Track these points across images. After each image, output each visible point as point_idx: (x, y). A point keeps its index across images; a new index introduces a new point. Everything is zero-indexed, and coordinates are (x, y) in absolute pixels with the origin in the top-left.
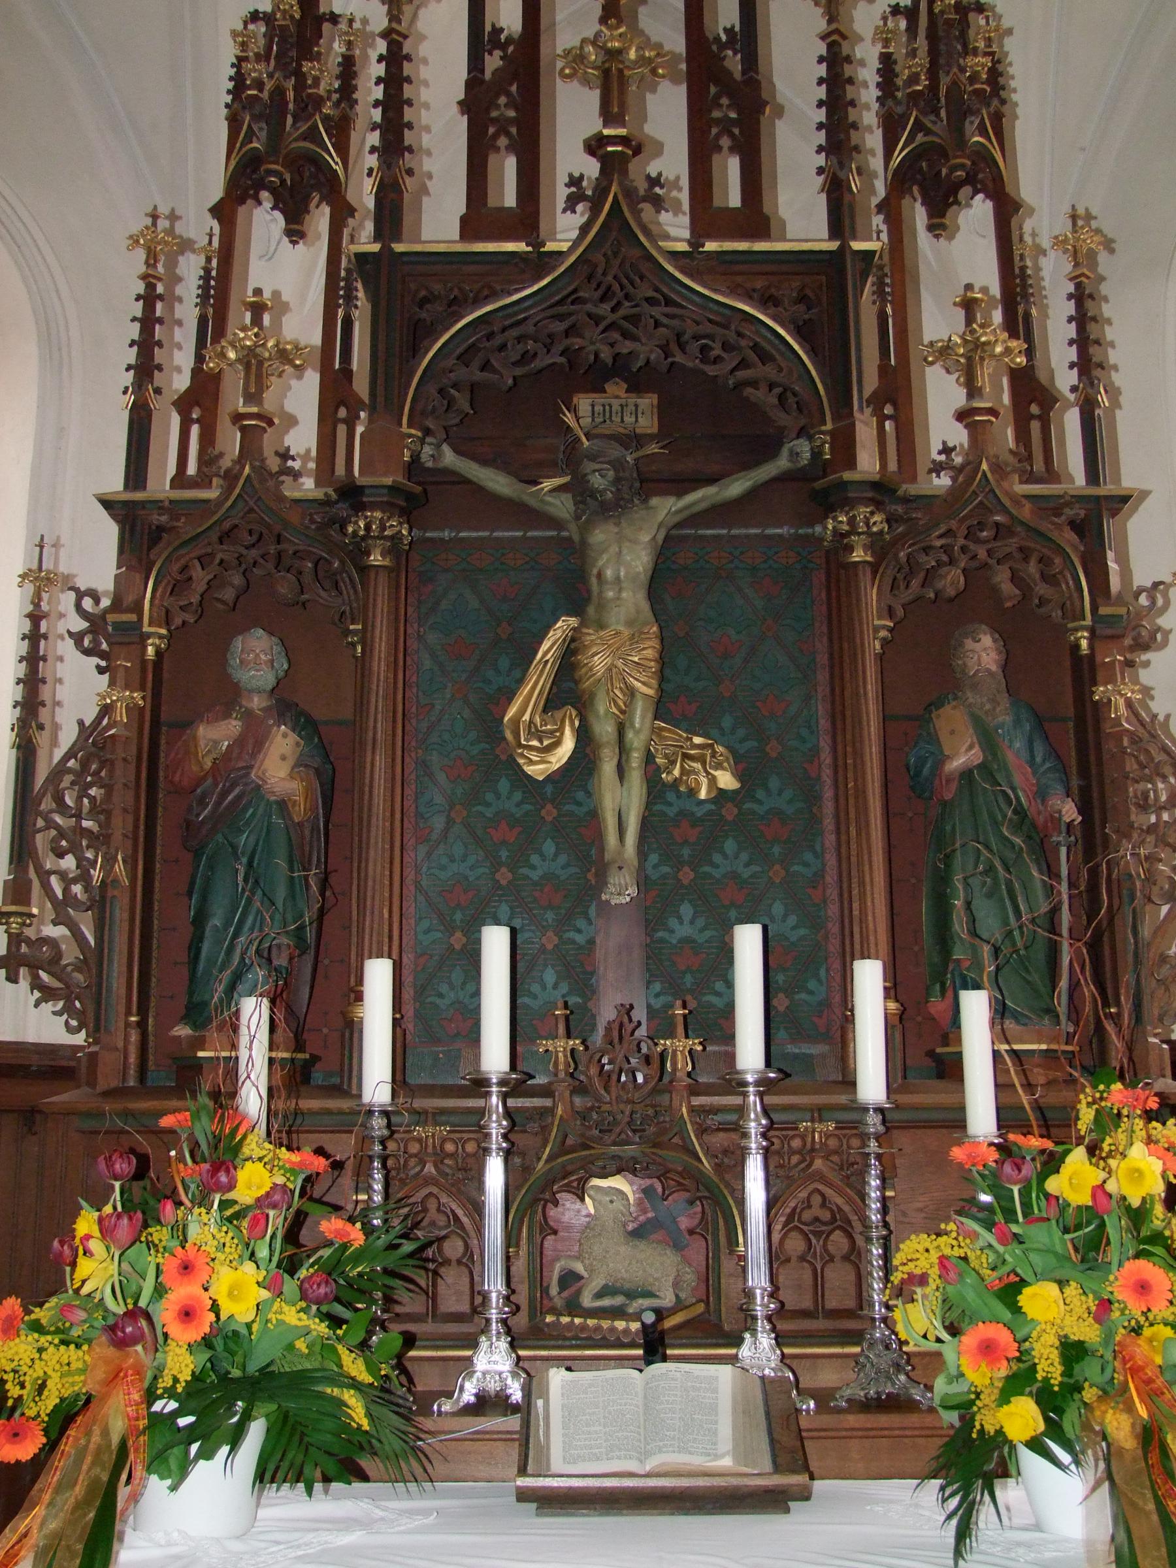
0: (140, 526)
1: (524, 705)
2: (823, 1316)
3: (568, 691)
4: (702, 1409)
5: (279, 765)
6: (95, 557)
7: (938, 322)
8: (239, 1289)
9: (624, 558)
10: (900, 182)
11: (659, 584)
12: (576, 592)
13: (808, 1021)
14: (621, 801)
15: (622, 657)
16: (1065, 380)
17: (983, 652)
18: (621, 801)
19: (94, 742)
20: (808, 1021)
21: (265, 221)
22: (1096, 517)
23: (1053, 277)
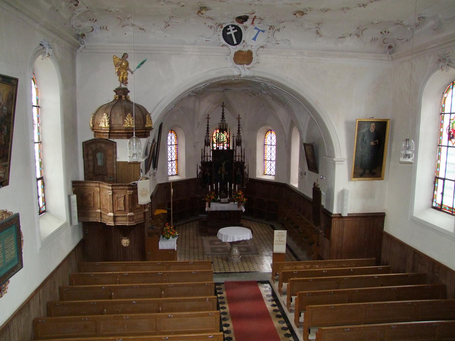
0: (202, 163)
1: (219, 171)
2: (231, 196)
3: (221, 170)
4: (226, 200)
5: (209, 175)
6: (200, 165)
7: (237, 155)
8: (213, 197)
9: (223, 164)
10: (236, 145)
11: (225, 166)
12: (221, 166)
13: (230, 186)
14: (223, 175)
15: (223, 170)
16: (243, 155)
17: (239, 169)
18: (223, 175)
19: (200, 173)
20: (230, 186)
21: (206, 147)
22: (244, 163)
23: (243, 151)
